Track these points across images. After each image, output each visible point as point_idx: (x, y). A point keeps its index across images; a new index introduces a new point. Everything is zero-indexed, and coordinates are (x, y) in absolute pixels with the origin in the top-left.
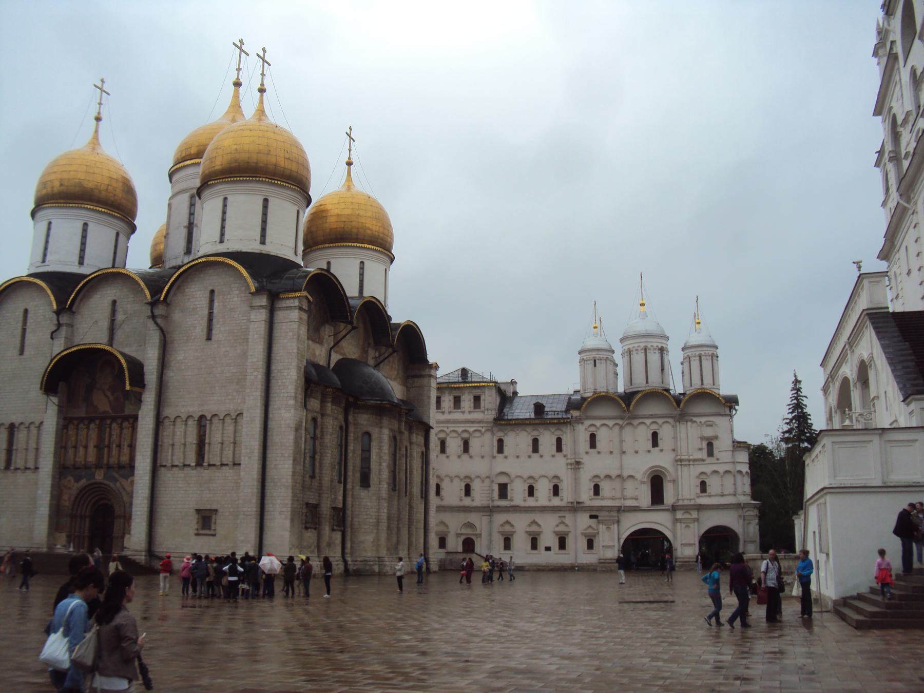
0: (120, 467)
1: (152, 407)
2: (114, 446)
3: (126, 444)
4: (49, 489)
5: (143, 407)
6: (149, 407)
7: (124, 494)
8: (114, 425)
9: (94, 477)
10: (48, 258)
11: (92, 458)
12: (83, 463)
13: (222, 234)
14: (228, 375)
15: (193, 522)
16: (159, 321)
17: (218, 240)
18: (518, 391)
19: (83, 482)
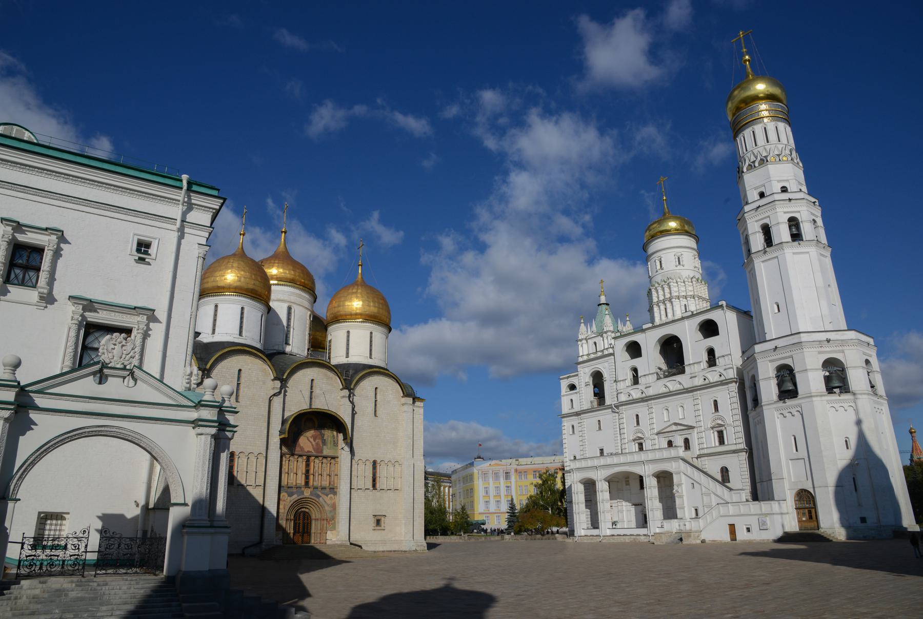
0: (323, 488)
2: (317, 474)
3: (325, 474)
7: (326, 505)
8: (317, 461)
9: (303, 494)
10: (244, 333)
11: (301, 480)
12: (294, 484)
13: (371, 354)
14: (388, 438)
15: (372, 522)
16: (351, 400)
17: (368, 355)
18: (279, 433)
19: (295, 497)
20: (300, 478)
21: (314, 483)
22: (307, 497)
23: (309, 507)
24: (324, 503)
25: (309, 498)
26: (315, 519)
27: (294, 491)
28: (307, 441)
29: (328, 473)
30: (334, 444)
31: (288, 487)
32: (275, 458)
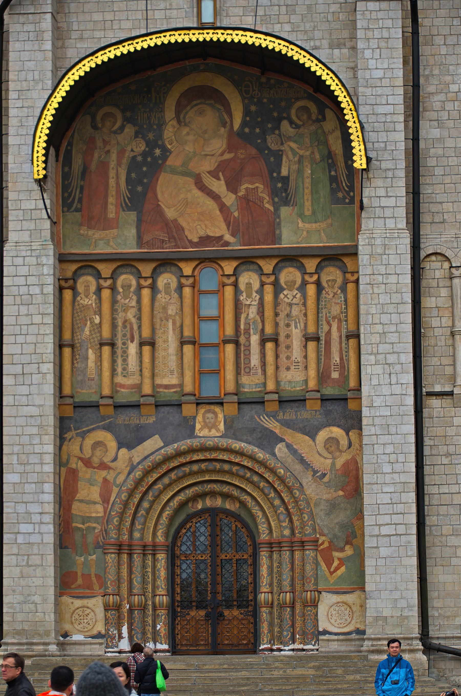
1: (402, 224)
2: (255, 339)
4: (49, 468)
5: (367, 224)
6: (390, 224)
9: (191, 434)
12: (147, 389)
20: (173, 362)
21: (245, 379)
22: (210, 443)
23: (236, 493)
24: (297, 467)
25: (216, 449)
26: (270, 544)
27: (144, 421)
28: (197, 193)
29: (311, 329)
30: (333, 192)
31: (117, 407)
32: (31, 280)
